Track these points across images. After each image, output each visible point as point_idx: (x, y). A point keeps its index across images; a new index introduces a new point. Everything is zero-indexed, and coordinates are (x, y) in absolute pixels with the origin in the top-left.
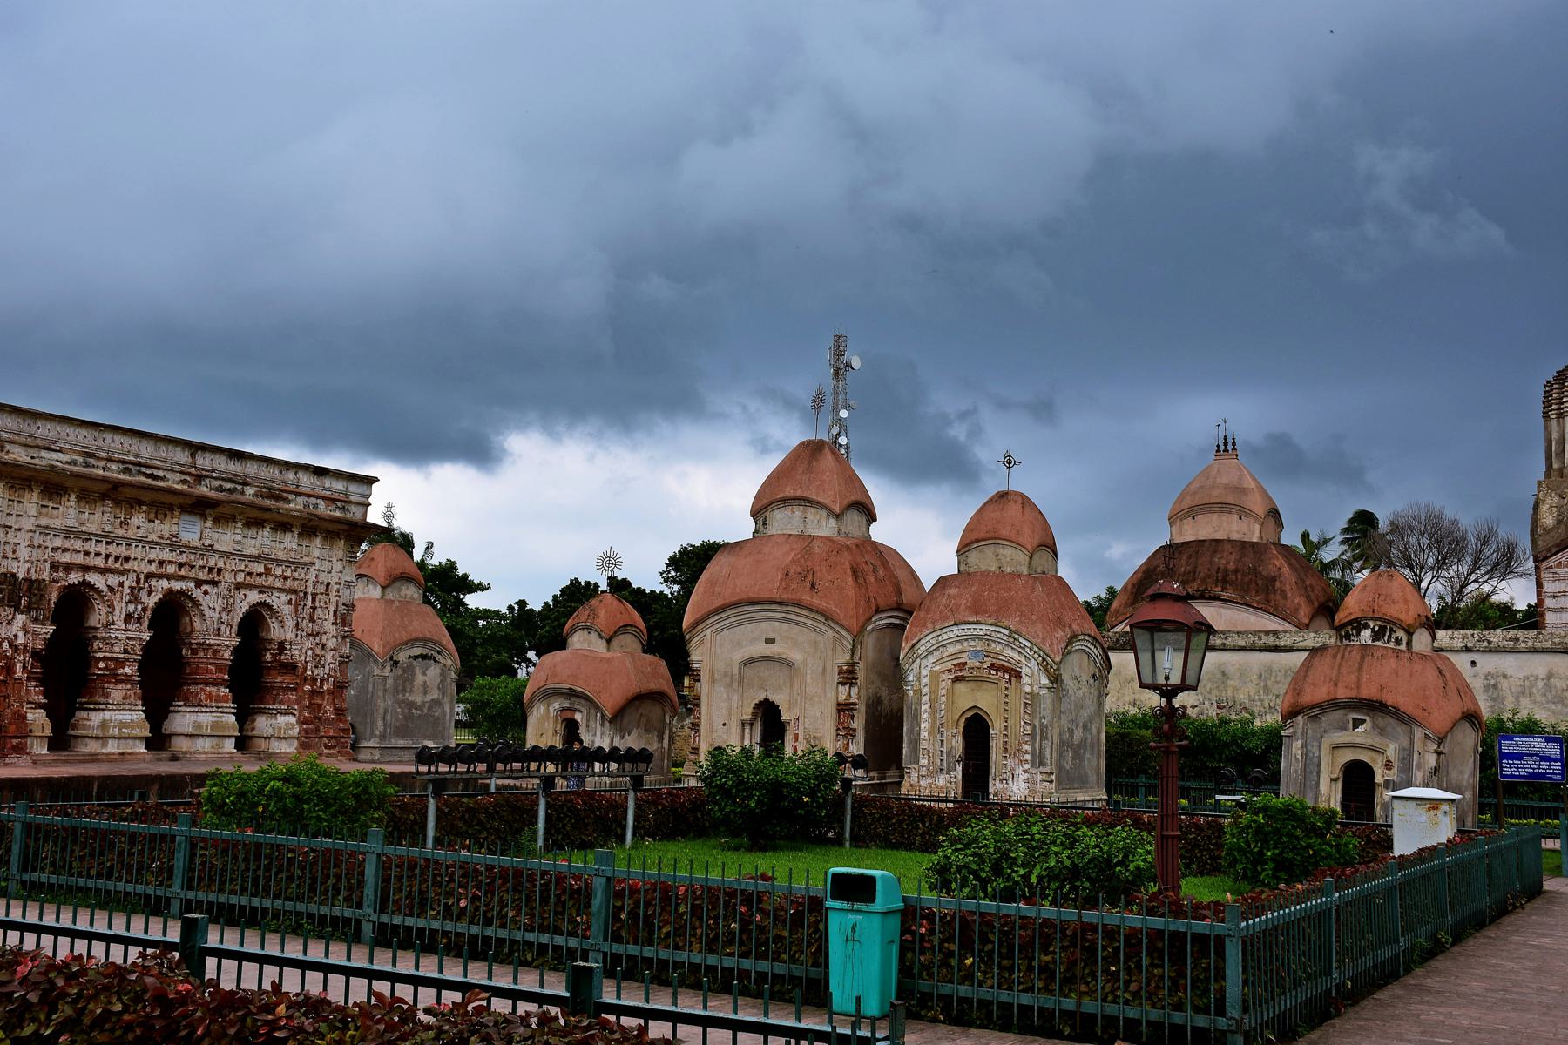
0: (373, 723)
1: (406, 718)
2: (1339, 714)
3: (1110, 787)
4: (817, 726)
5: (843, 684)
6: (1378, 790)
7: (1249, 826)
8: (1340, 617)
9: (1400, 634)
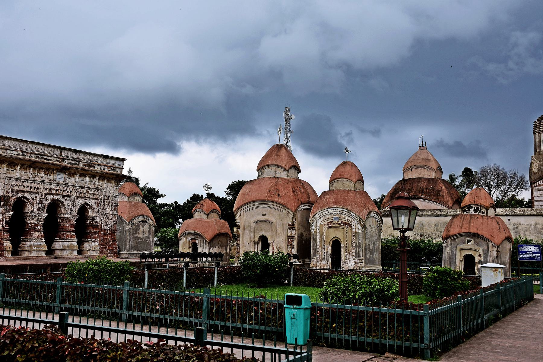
0: (125, 244)
1: (137, 243)
2: (463, 238)
3: (383, 265)
4: (281, 244)
5: (290, 229)
6: (476, 264)
7: (431, 278)
8: (463, 204)
9: (484, 210)
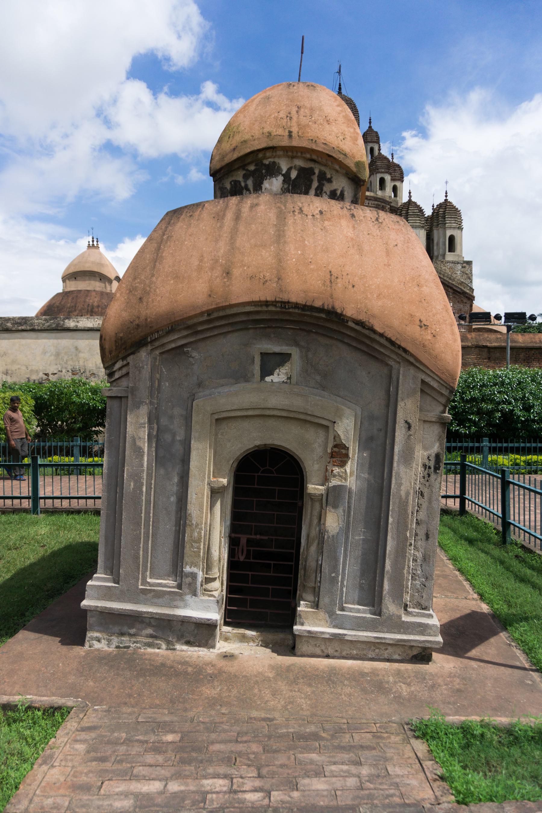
2: (229, 344)
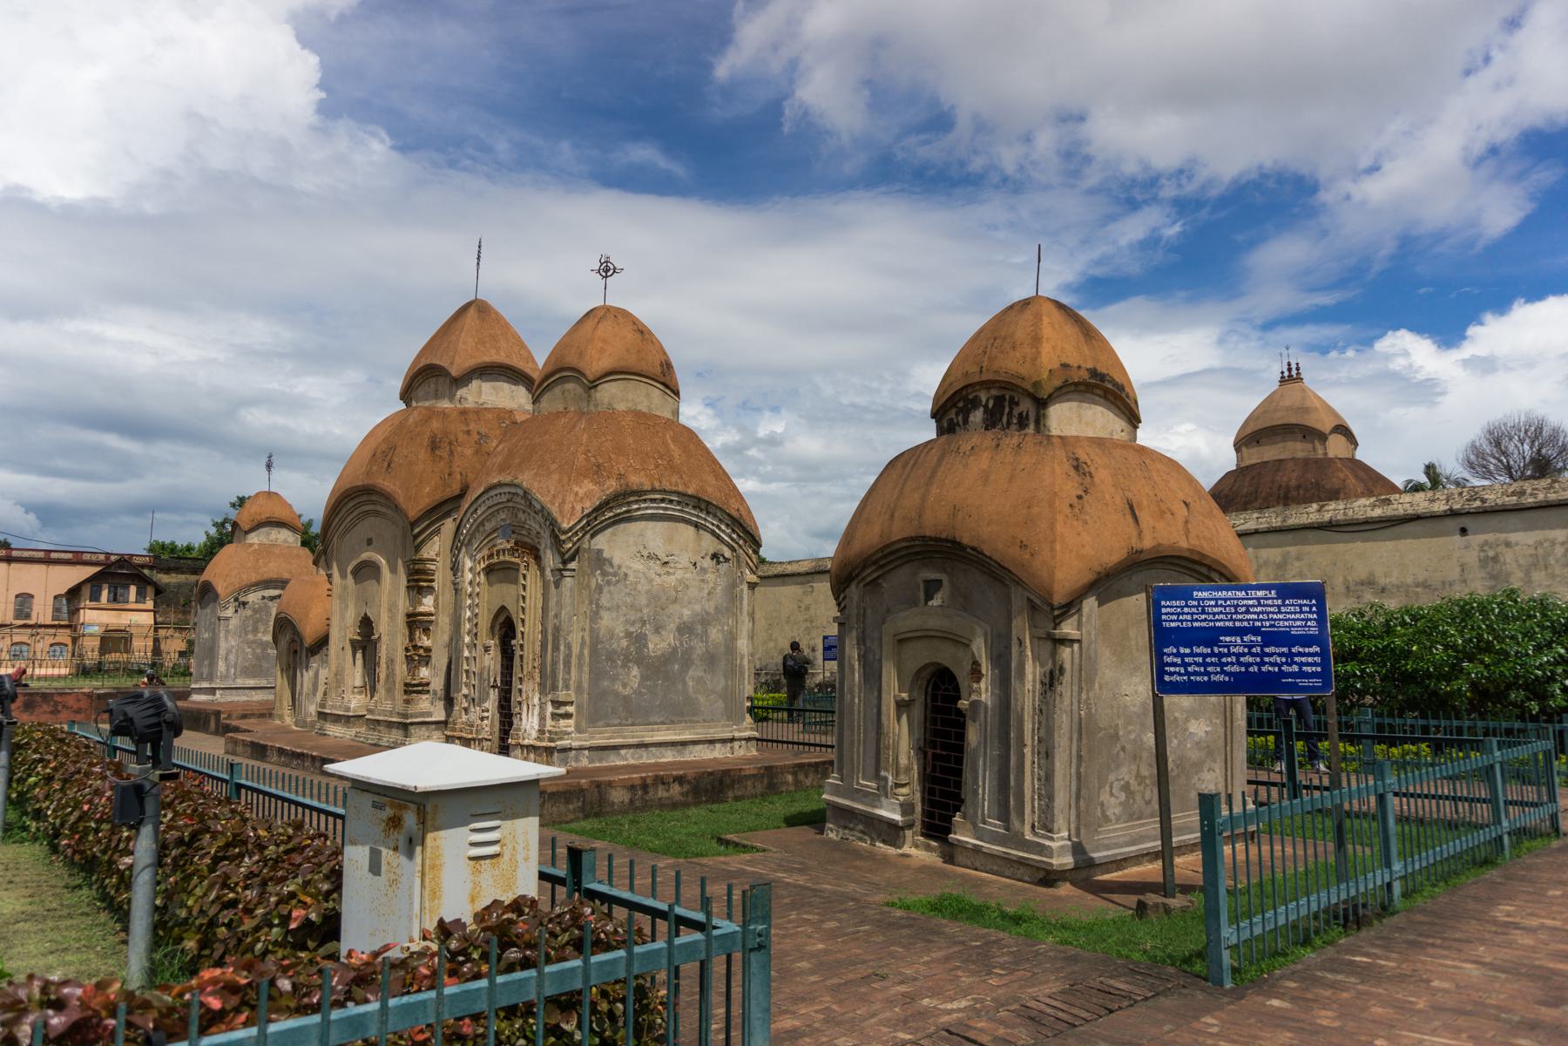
1: (258, 658)
